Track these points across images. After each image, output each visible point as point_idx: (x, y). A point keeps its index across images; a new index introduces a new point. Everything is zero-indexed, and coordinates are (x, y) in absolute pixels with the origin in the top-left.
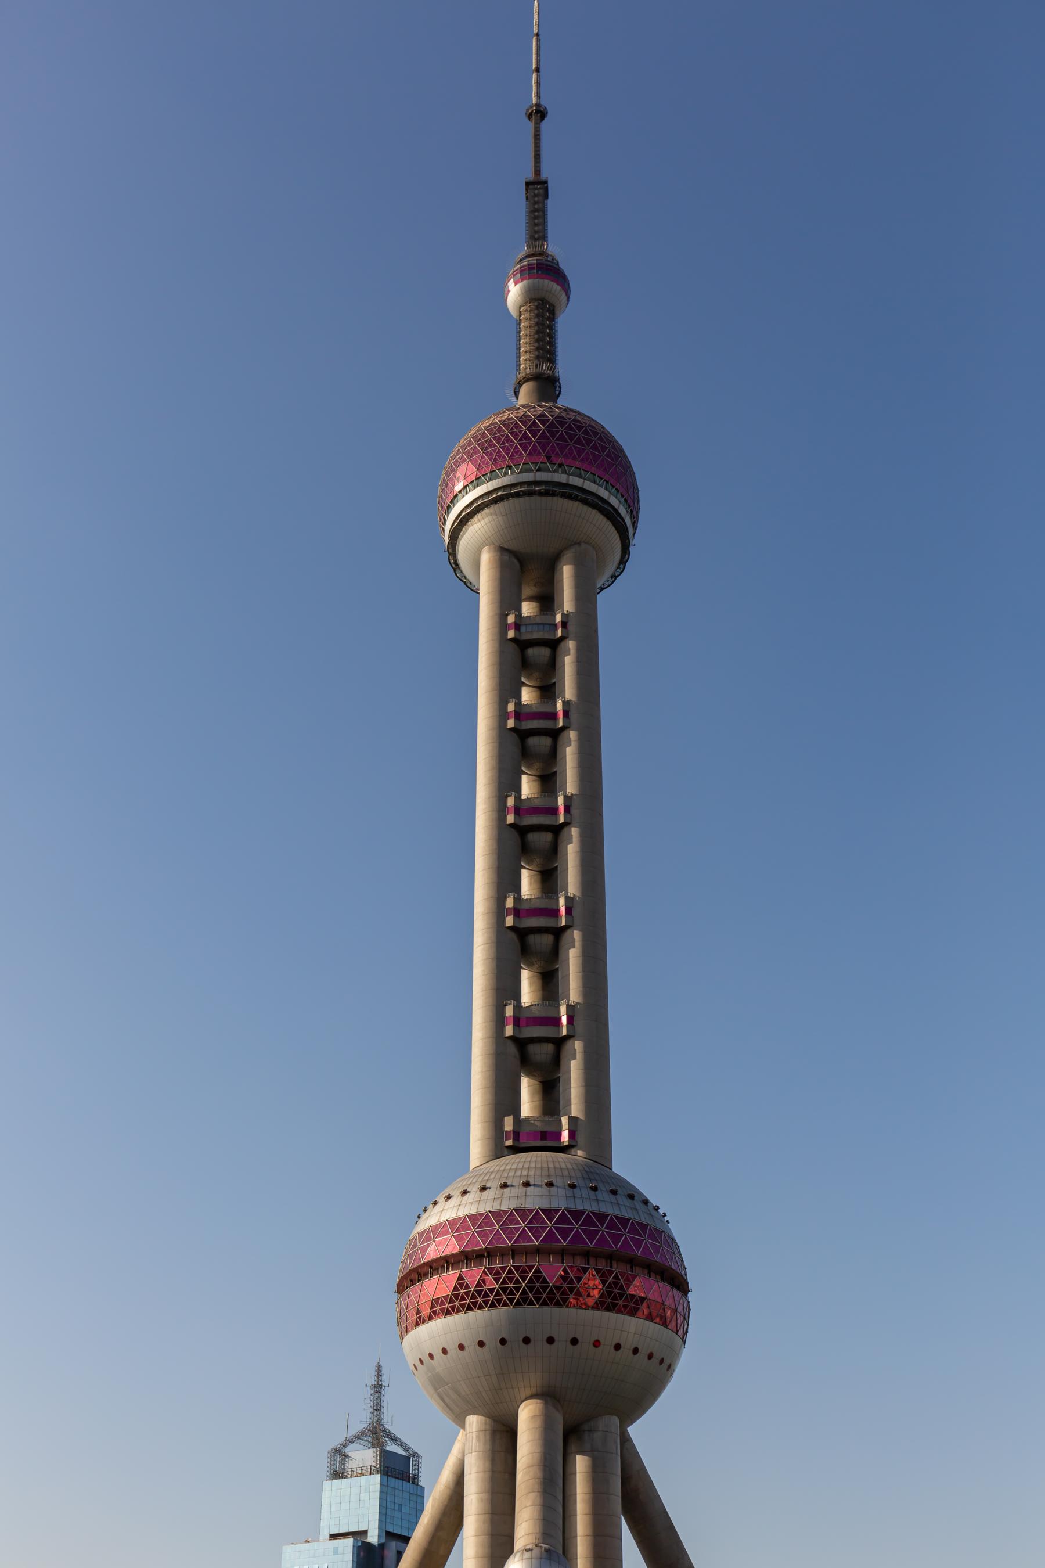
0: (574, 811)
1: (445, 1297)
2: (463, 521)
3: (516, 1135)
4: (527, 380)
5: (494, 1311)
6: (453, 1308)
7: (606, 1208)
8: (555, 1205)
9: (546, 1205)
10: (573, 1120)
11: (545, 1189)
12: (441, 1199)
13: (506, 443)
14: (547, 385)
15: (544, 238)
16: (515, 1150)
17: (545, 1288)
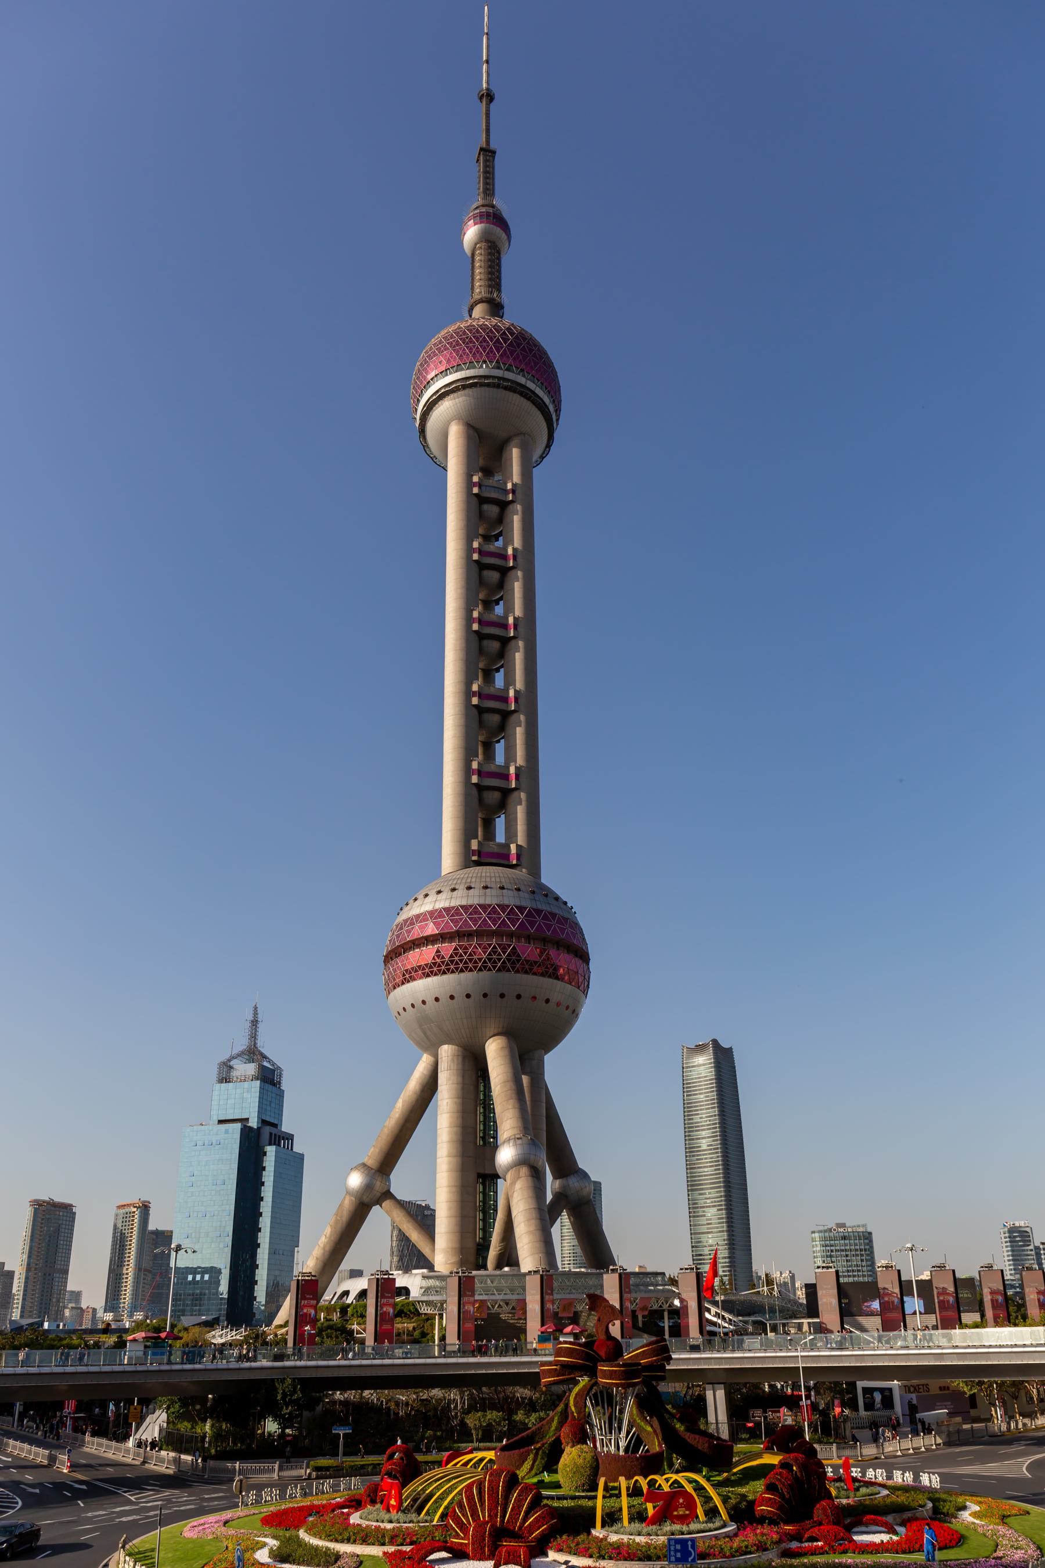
0: (521, 629)
1: (426, 965)
2: (440, 396)
3: (479, 853)
4: (481, 301)
5: (462, 975)
6: (432, 972)
7: (544, 907)
8: (506, 902)
9: (482, 902)
10: (519, 847)
11: (516, 893)
12: (421, 897)
13: (471, 345)
14: (496, 308)
15: (493, 194)
16: (478, 863)
17: (518, 961)
